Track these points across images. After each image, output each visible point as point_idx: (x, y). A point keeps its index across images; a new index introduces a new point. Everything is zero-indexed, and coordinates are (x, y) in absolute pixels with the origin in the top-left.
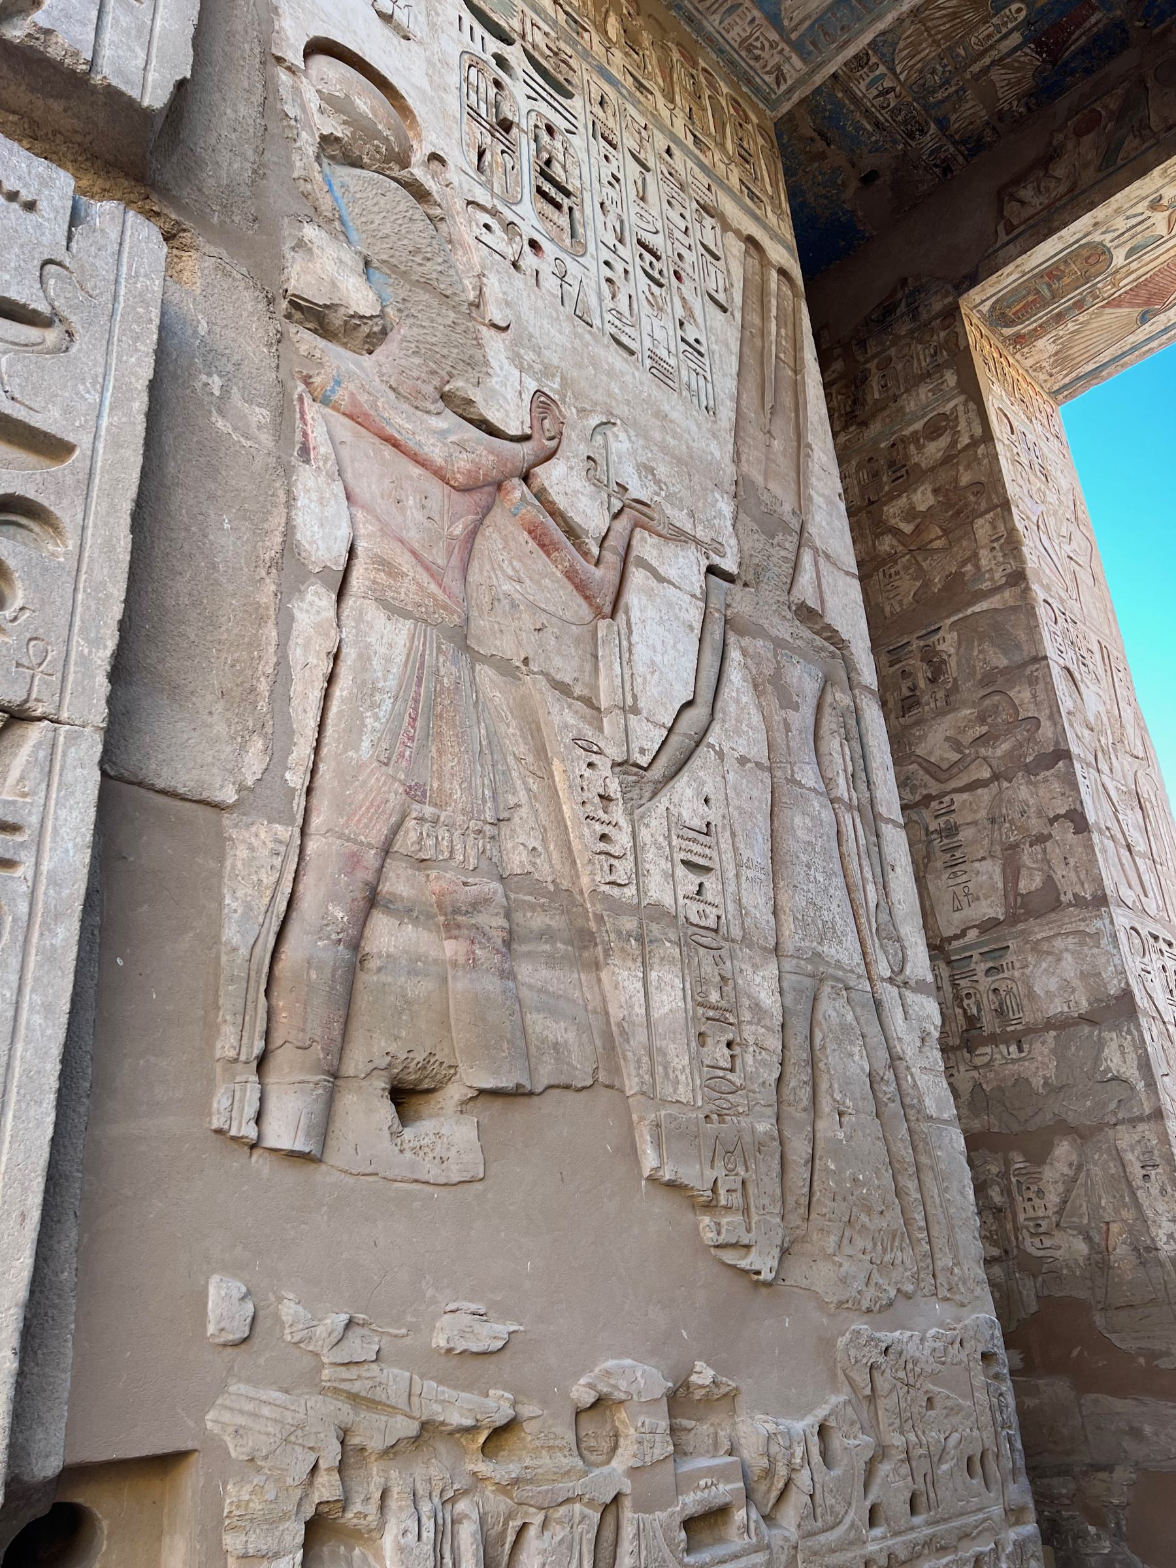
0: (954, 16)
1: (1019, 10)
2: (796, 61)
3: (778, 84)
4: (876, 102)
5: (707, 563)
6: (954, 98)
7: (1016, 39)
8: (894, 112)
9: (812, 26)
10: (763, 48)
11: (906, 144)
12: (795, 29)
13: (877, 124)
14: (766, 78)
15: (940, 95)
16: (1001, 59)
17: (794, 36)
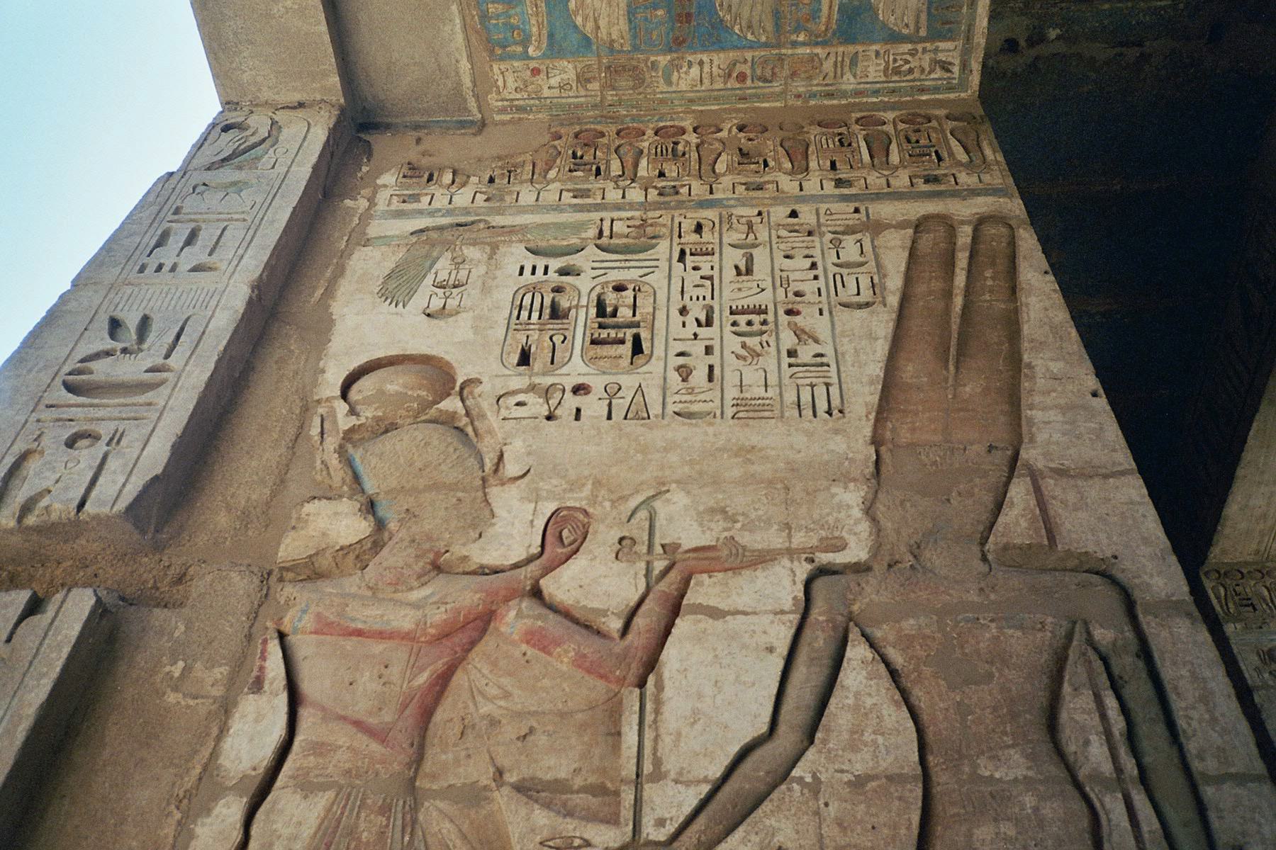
2: (942, 45)
3: (948, 71)
5: (809, 567)
9: (929, 13)
10: (907, 62)
12: (918, 29)
14: (933, 76)
17: (923, 33)
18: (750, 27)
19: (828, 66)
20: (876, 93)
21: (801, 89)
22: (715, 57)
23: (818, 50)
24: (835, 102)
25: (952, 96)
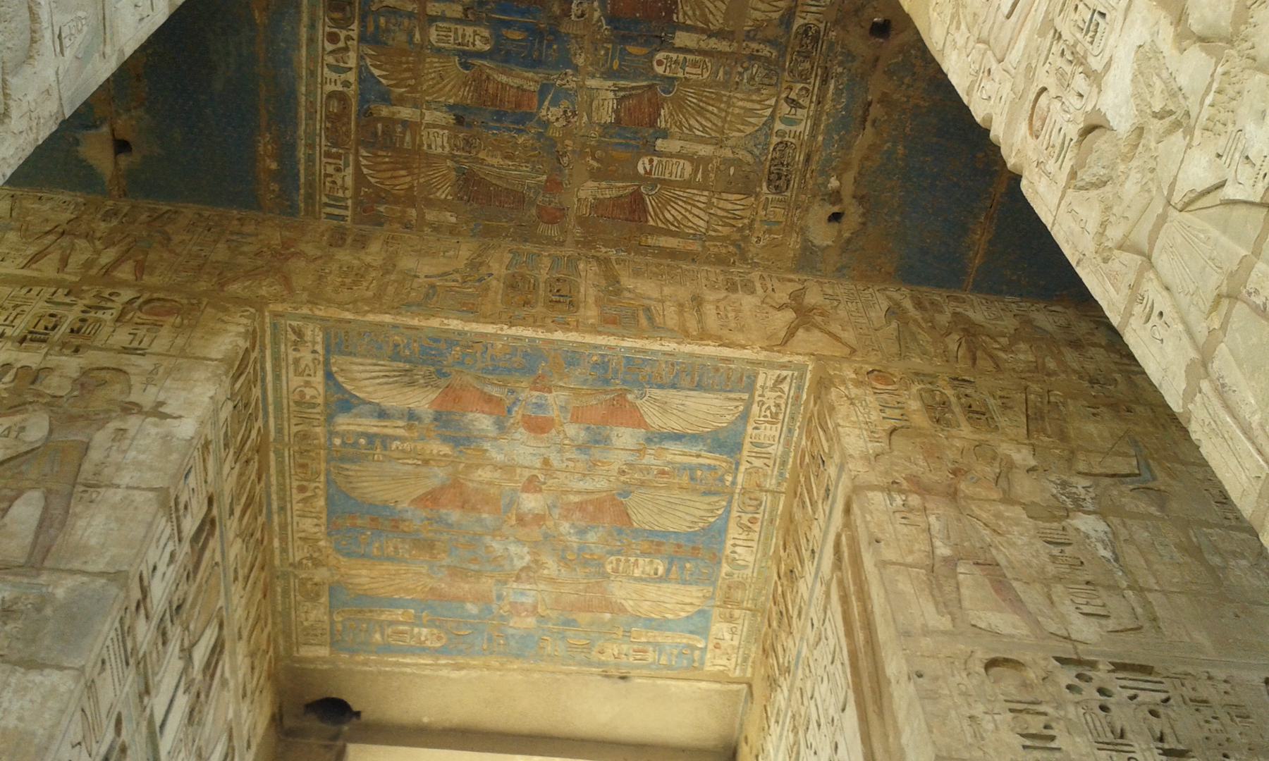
0: (701, 112)
1: (660, 63)
2: (760, 382)
4: (807, 104)
6: (760, 35)
7: (682, 39)
8: (804, 77)
10: (769, 408)
11: (826, 33)
13: (825, 81)
14: (786, 390)
15: (766, 51)
16: (703, 31)
17: (746, 396)
18: (712, 511)
19: (758, 463)
20: (790, 431)
21: (774, 481)
22: (730, 536)
23: (742, 468)
24: (791, 460)
25: (809, 375)
